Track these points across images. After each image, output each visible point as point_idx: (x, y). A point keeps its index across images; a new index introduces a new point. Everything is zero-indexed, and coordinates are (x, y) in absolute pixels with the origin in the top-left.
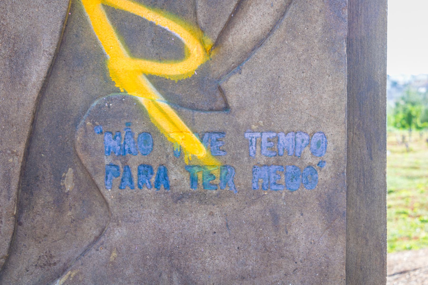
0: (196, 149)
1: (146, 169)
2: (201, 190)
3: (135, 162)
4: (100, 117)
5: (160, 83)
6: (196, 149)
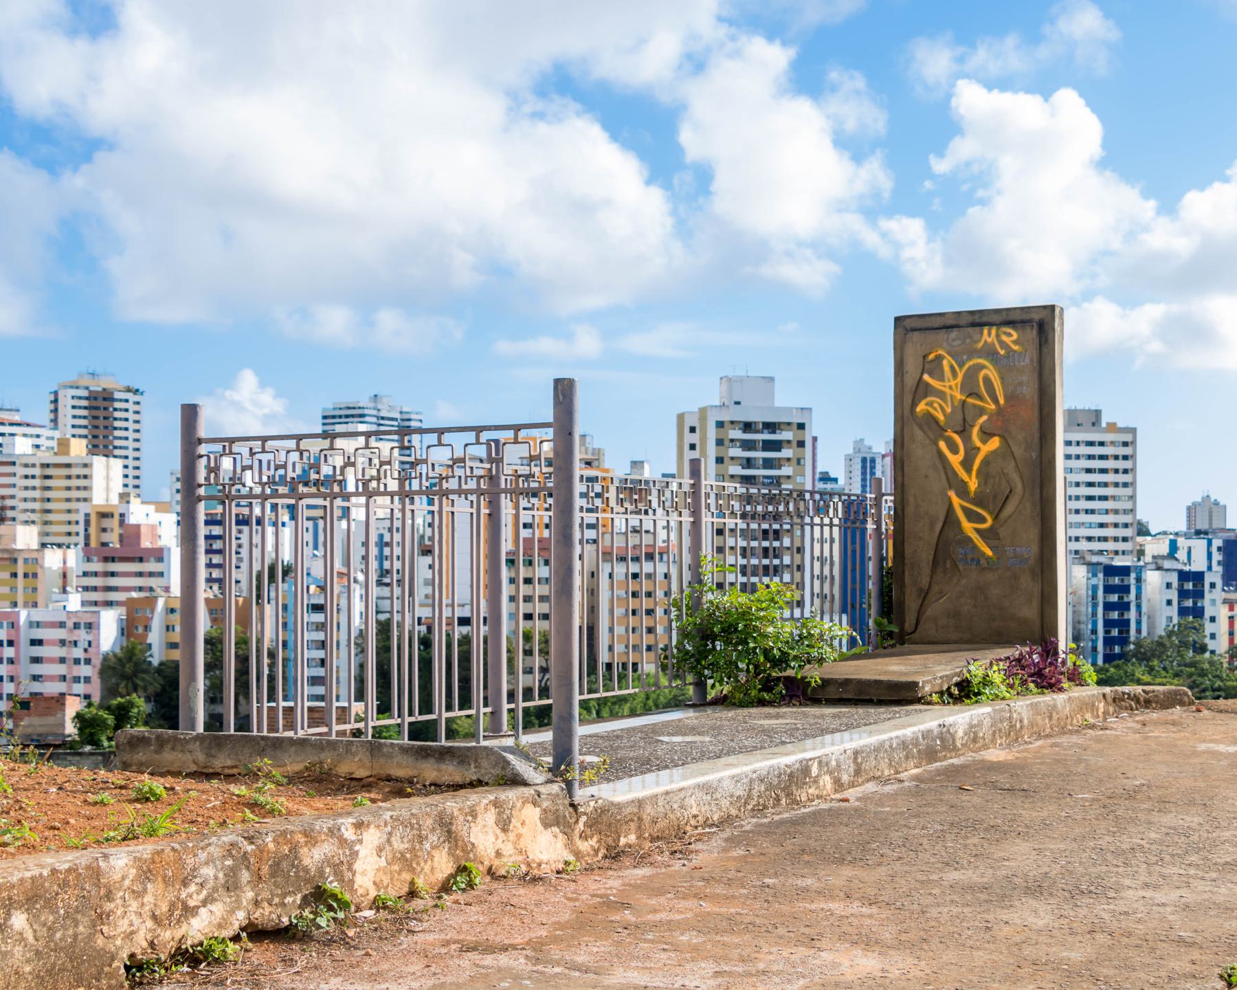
0: (989, 553)
1: (973, 559)
2: (990, 566)
3: (969, 557)
5: (978, 531)
6: (989, 553)
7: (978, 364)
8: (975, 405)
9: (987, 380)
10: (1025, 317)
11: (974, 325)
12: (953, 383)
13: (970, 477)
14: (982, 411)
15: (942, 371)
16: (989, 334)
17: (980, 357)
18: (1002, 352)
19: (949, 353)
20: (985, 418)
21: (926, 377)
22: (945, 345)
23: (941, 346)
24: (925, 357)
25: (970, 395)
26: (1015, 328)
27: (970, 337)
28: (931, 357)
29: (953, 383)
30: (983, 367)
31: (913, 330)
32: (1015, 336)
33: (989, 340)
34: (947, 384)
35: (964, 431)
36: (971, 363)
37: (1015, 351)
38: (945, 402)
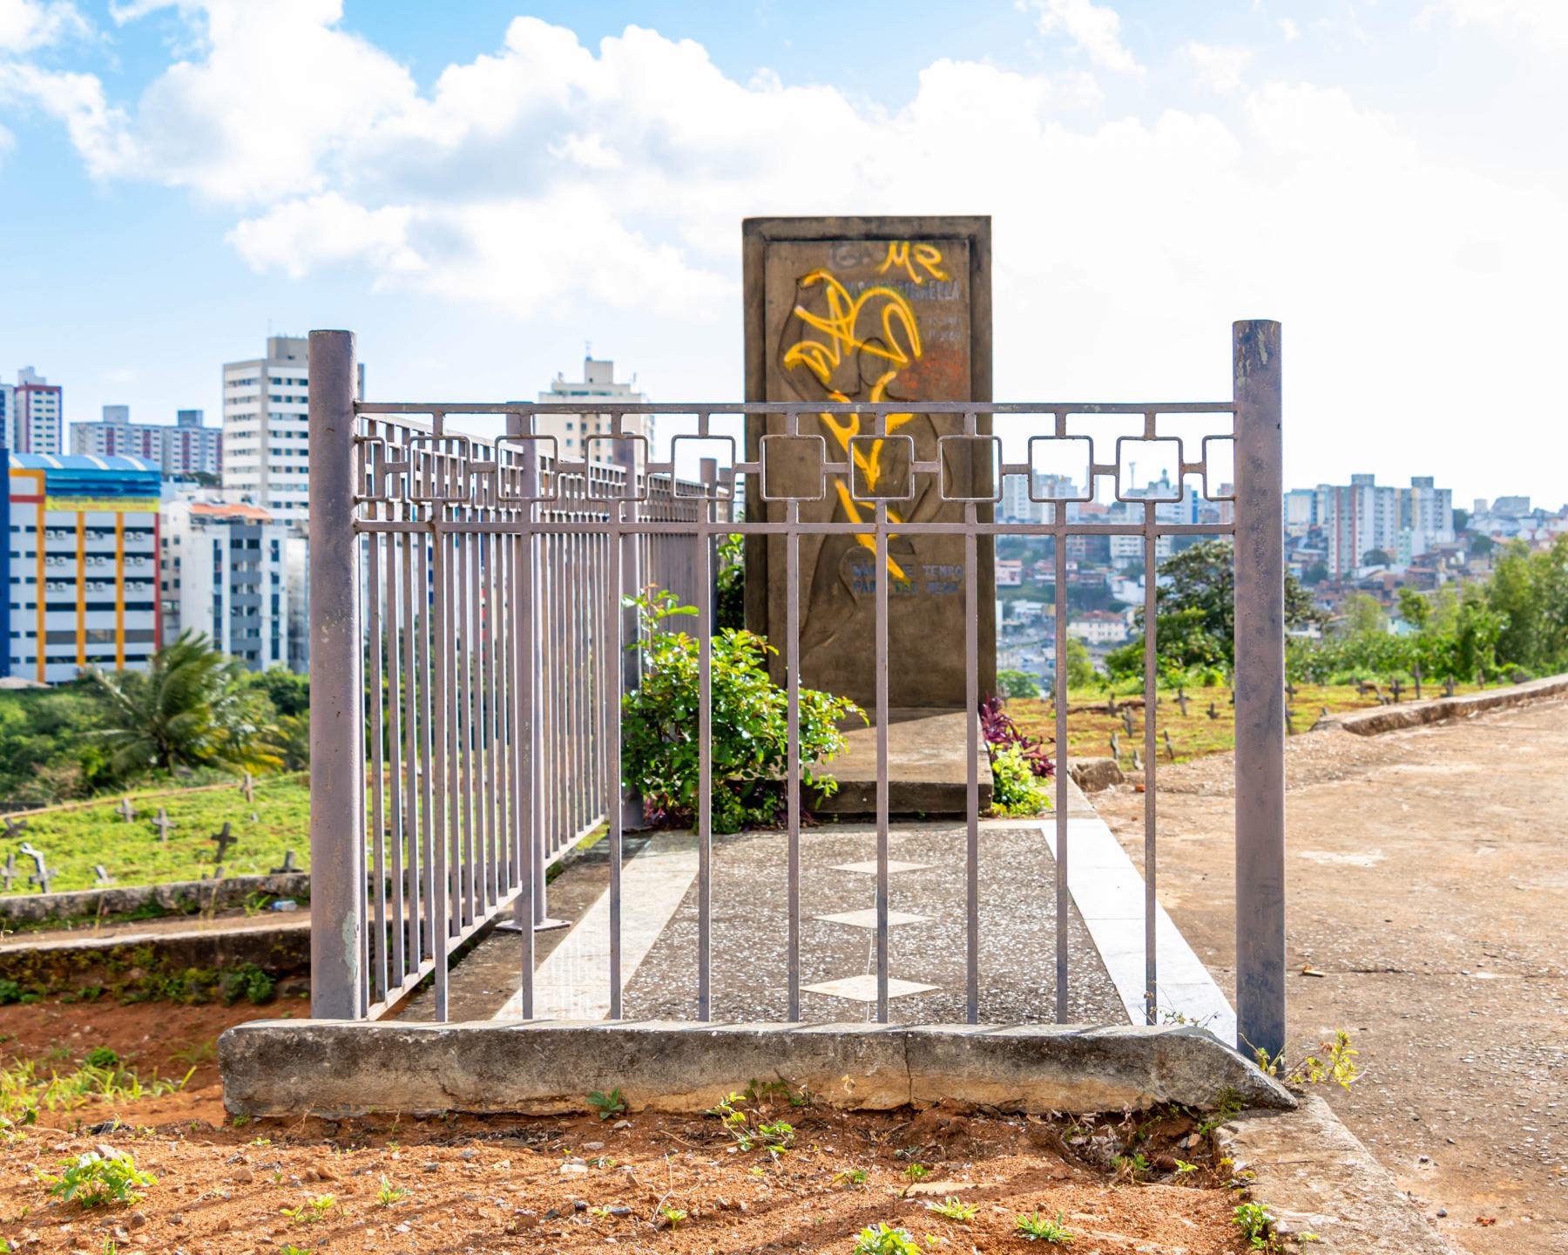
4: (852, 557)
7: (882, 296)
8: (875, 357)
9: (895, 321)
10: (948, 230)
12: (842, 322)
13: (868, 461)
14: (887, 365)
15: (826, 302)
16: (899, 253)
17: (884, 285)
18: (918, 280)
19: (837, 278)
21: (800, 311)
22: (830, 264)
23: (824, 267)
24: (798, 281)
25: (869, 341)
26: (937, 246)
27: (870, 255)
28: (808, 281)
29: (842, 322)
30: (889, 300)
32: (937, 257)
33: (899, 261)
34: (834, 323)
35: (857, 395)
36: (870, 293)
37: (937, 280)
38: (831, 349)
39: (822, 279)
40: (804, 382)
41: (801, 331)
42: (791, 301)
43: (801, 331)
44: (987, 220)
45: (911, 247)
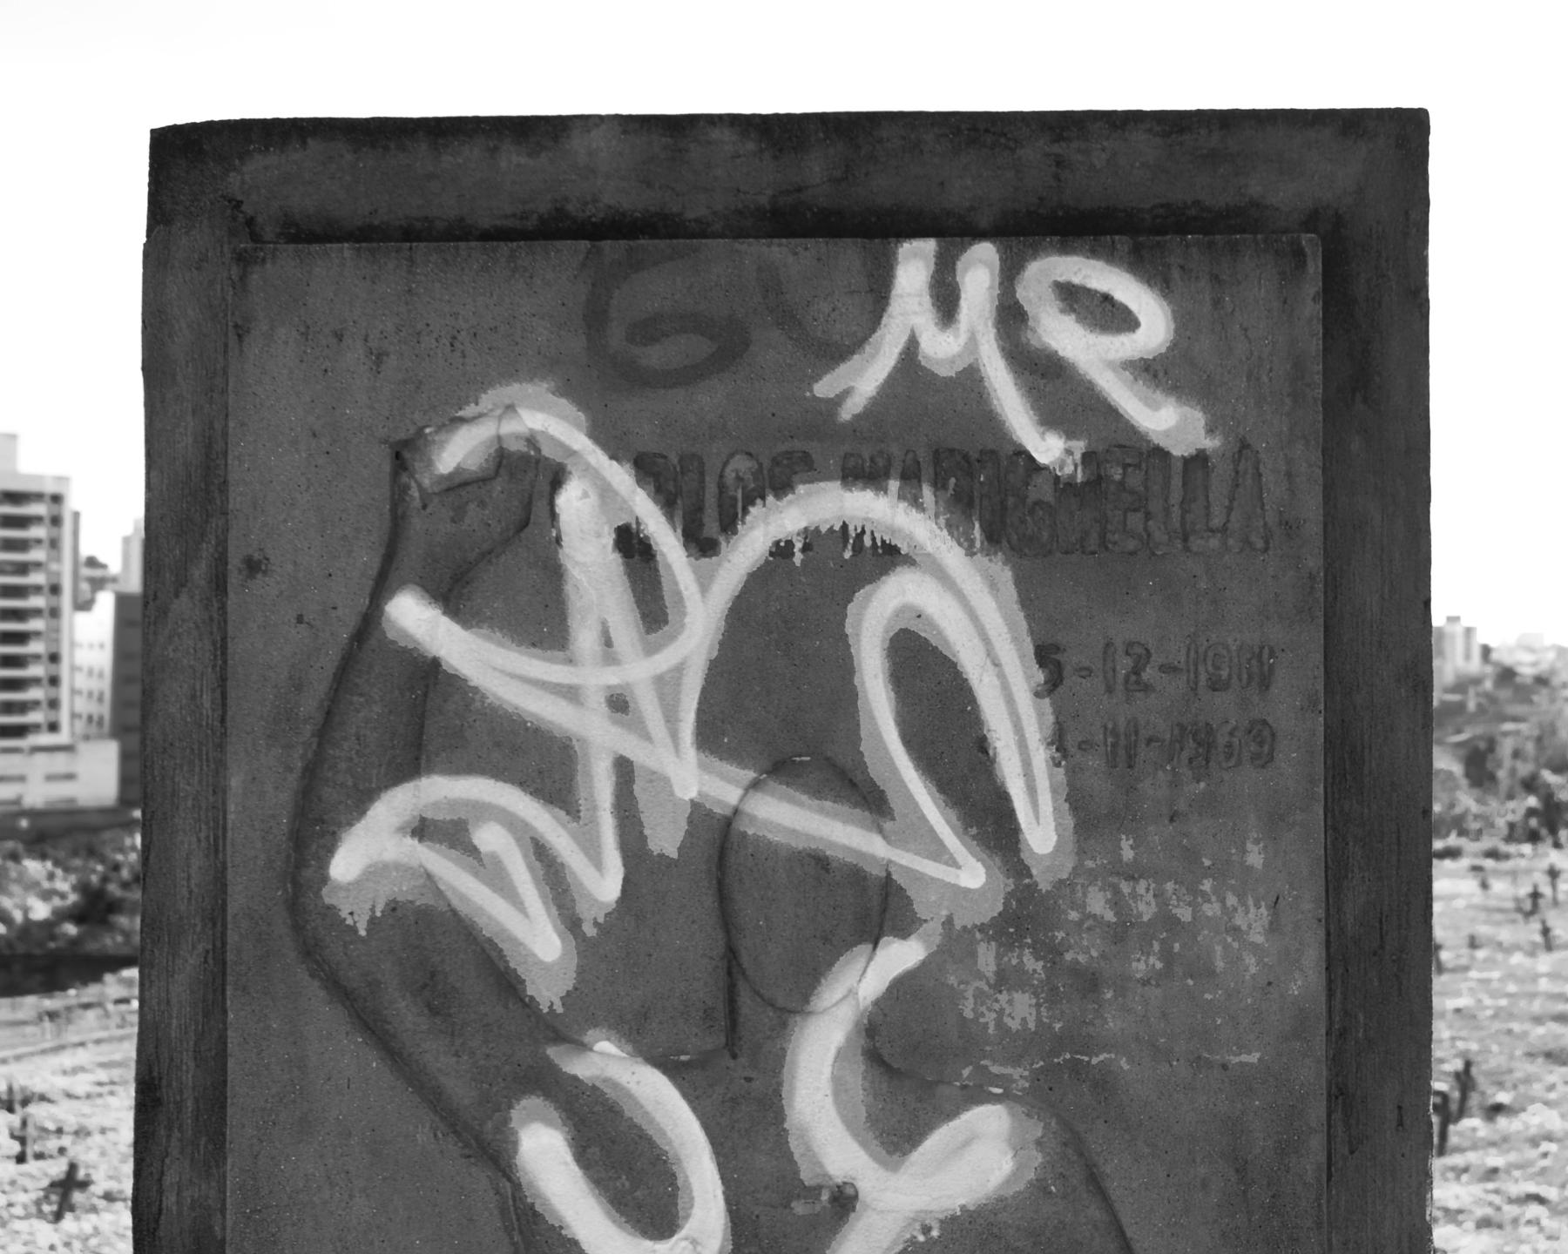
8: (817, 865)
9: (921, 664)
11: (786, 220)
12: (638, 670)
14: (878, 907)
15: (554, 573)
16: (946, 300)
18: (1048, 449)
20: (900, 956)
21: (412, 615)
24: (404, 455)
29: (638, 670)
30: (888, 556)
31: (310, 233)
32: (1155, 323)
33: (942, 349)
39: (531, 440)
40: (434, 993)
41: (429, 721)
42: (367, 559)
43: (429, 721)
44: (1405, 133)
45: (1010, 273)
